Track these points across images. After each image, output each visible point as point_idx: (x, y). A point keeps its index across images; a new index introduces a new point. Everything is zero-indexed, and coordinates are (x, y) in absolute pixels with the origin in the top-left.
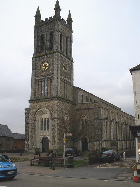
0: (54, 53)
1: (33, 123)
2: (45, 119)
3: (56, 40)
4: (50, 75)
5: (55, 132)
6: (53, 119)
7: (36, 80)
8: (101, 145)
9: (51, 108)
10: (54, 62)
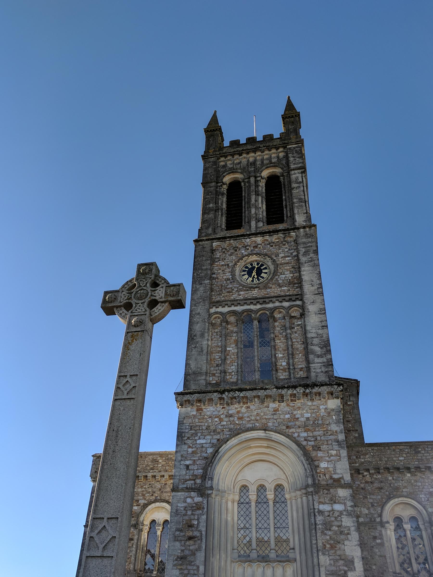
1: (198, 507)
2: (261, 488)
3: (302, 193)
6: (328, 487)
9: (305, 434)
10: (303, 259)
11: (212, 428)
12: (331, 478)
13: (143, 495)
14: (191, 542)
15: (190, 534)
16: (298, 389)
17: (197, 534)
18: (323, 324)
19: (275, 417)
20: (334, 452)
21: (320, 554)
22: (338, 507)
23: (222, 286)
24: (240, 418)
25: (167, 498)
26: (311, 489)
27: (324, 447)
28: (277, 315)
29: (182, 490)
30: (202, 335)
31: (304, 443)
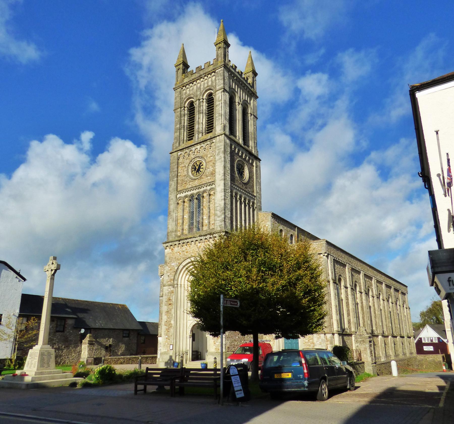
0: (216, 137)
1: (172, 292)
7: (179, 197)
8: (329, 343)
11: (177, 258)
15: (170, 303)
17: (172, 302)
28: (205, 195)
30: (174, 211)
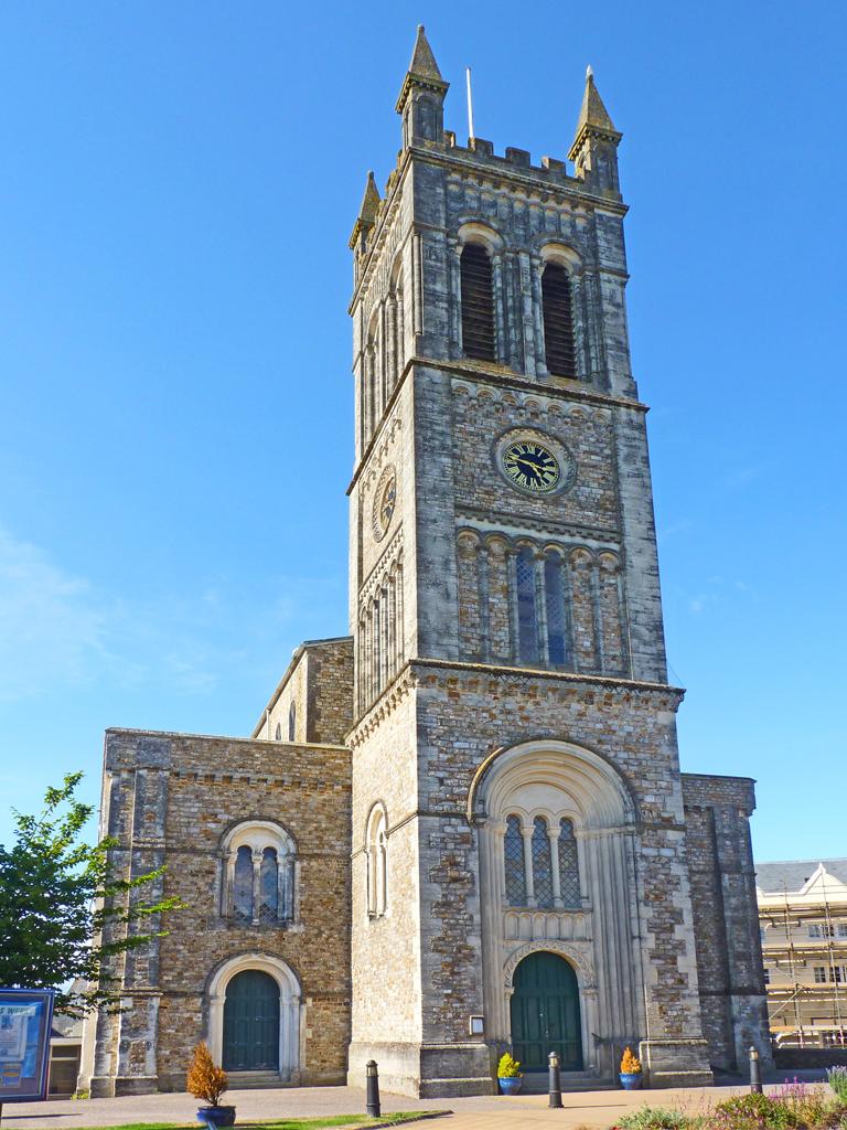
1: (465, 839)
2: (541, 821)
4: (589, 536)
5: (677, 916)
6: (655, 827)
9: (624, 755)
10: (624, 468)
12: (659, 816)
13: (227, 807)
14: (457, 885)
16: (619, 689)
18: (654, 592)
19: (581, 724)
20: (664, 784)
21: (642, 904)
22: (666, 852)
23: (473, 476)
24: (526, 719)
25: (274, 815)
26: (631, 828)
27: (651, 776)
29: (437, 814)
31: (624, 767)
